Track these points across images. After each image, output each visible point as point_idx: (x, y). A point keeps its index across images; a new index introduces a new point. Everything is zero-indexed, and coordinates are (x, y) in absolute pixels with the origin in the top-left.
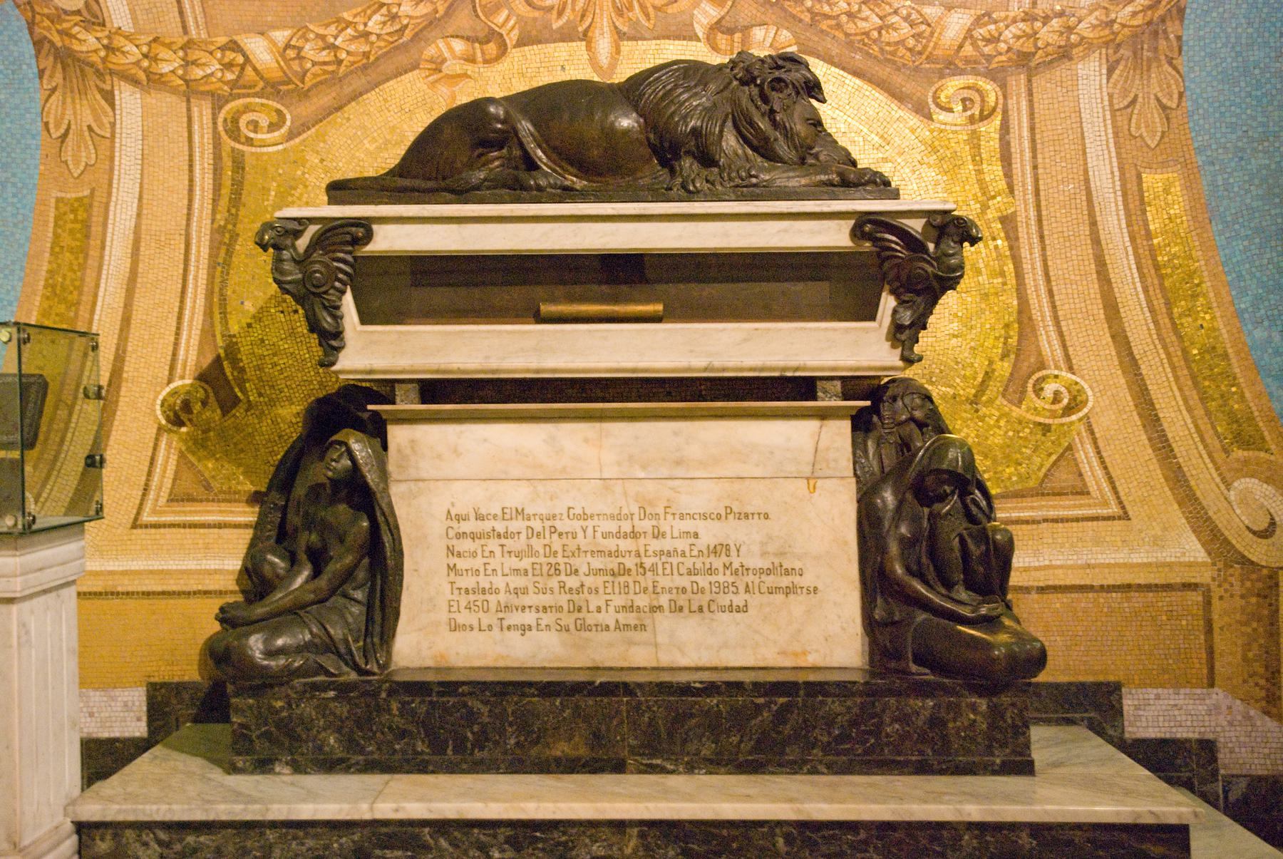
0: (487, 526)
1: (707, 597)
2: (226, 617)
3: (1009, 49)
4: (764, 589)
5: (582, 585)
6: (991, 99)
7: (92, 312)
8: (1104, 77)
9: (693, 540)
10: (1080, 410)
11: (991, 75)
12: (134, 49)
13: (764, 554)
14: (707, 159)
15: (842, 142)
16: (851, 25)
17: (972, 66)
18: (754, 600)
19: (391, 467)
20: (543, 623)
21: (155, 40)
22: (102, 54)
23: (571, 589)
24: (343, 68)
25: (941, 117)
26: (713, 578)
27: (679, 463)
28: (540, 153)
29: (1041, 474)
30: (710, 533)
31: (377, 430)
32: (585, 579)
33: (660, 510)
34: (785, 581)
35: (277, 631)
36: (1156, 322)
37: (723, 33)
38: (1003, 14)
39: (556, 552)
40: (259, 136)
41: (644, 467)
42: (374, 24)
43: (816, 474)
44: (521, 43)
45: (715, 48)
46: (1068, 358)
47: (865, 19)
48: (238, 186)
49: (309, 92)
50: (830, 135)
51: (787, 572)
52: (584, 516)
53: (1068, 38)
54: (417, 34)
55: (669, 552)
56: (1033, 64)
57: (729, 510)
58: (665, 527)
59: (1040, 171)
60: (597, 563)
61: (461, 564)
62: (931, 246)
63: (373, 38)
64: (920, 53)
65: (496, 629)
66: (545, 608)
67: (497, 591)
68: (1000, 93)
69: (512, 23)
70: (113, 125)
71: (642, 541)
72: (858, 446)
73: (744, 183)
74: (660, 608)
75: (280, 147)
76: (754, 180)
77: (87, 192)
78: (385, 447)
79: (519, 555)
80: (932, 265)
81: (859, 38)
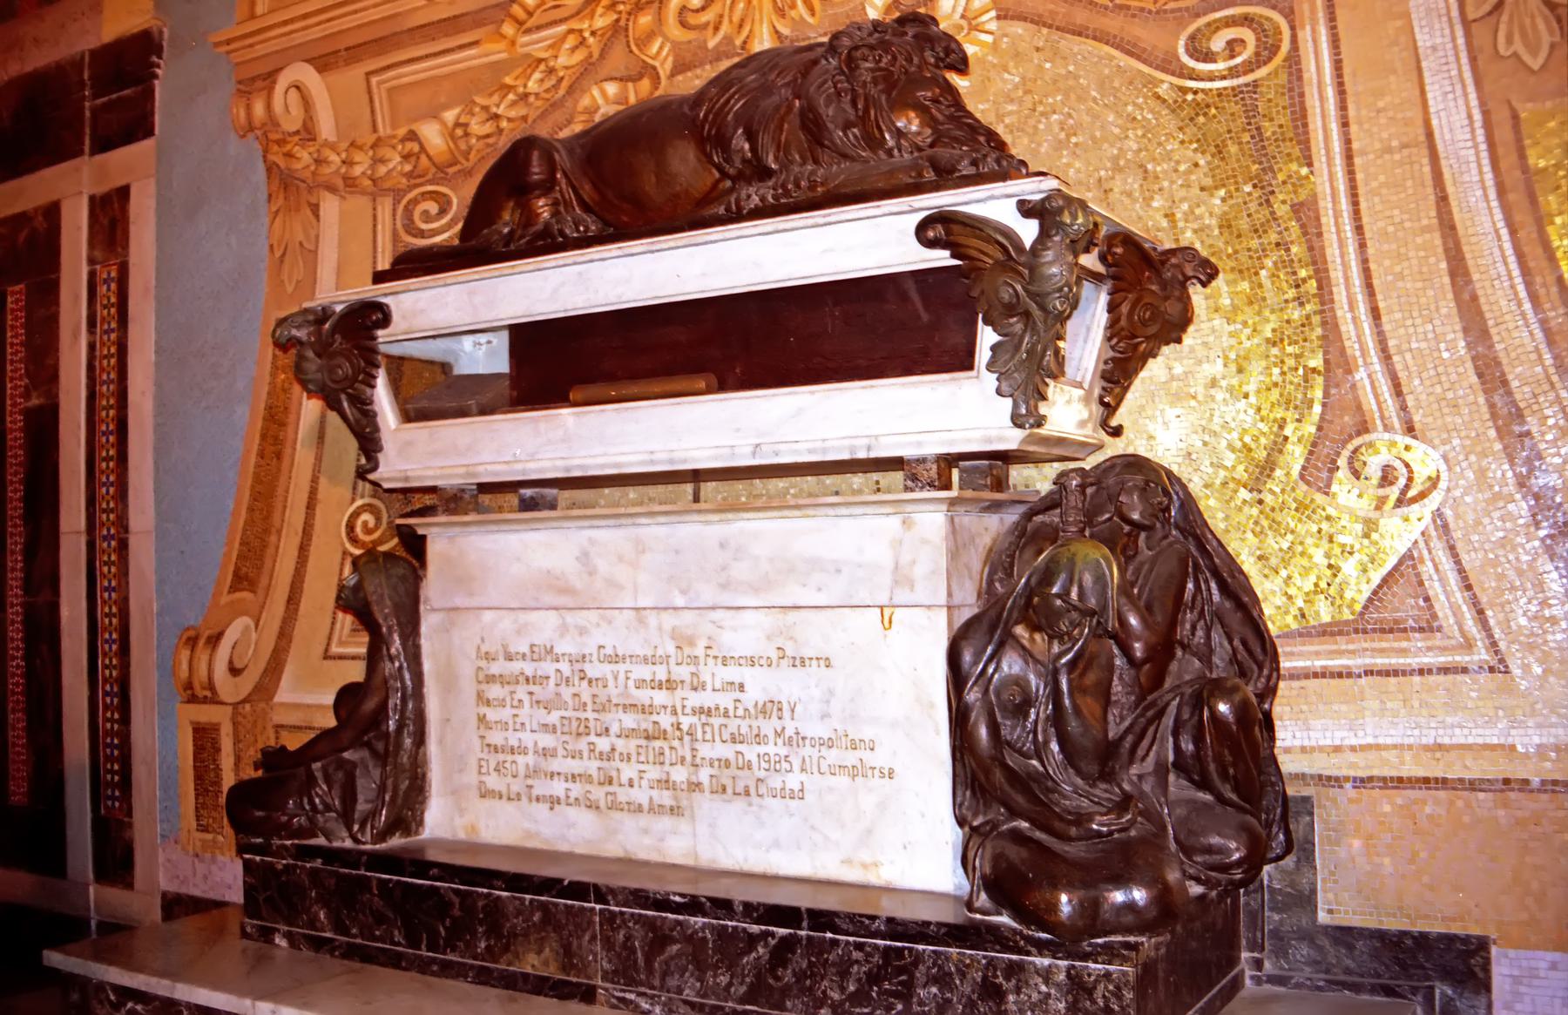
4: (824, 768)
5: (613, 749)
9: (738, 695)
23: (601, 753)
26: (762, 749)
39: (585, 704)
43: (896, 601)
55: (709, 710)
60: (630, 721)
65: (524, 798)
66: (573, 776)
67: (525, 752)
71: (679, 693)
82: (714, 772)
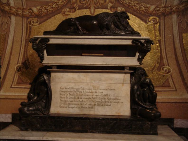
0: (67, 90)
1: (104, 103)
2: (22, 104)
3: (161, 12)
6: (158, 20)
7: (5, 52)
8: (177, 17)
10: (170, 73)
11: (158, 16)
12: (14, 10)
13: (114, 96)
14: (108, 29)
15: (132, 27)
16: (135, 8)
17: (154, 15)
18: (112, 104)
19: (51, 80)
20: (76, 107)
21: (18, 8)
22: (9, 10)
24: (48, 13)
25: (149, 23)
26: (105, 100)
27: (100, 80)
28: (80, 27)
29: (163, 83)
30: (105, 92)
31: (49, 74)
32: (83, 99)
33: (97, 88)
34: (117, 101)
35: (30, 107)
36: (183, 58)
37: (113, 8)
38: (160, 6)
40: (34, 24)
41: (94, 81)
42: (54, 6)
44: (79, 9)
45: (111, 11)
46: (168, 64)
47: (137, 6)
48: (30, 32)
49: (43, 17)
50: (130, 26)
51: (118, 99)
52: (83, 89)
53: (171, 10)
54: (61, 8)
56: (165, 15)
57: (108, 89)
58: (97, 91)
59: (165, 33)
60: (85, 97)
61: (62, 96)
62: (145, 45)
63: (54, 8)
64: (146, 12)
68: (159, 20)
69: (77, 6)
70: (10, 22)
71: (93, 93)
72: (131, 78)
73: (114, 33)
74: (96, 105)
75: (37, 26)
76: (116, 33)
77: (6, 33)
78: (50, 76)
79: (72, 95)
80: (145, 48)
81: (136, 10)
82: (98, 103)
